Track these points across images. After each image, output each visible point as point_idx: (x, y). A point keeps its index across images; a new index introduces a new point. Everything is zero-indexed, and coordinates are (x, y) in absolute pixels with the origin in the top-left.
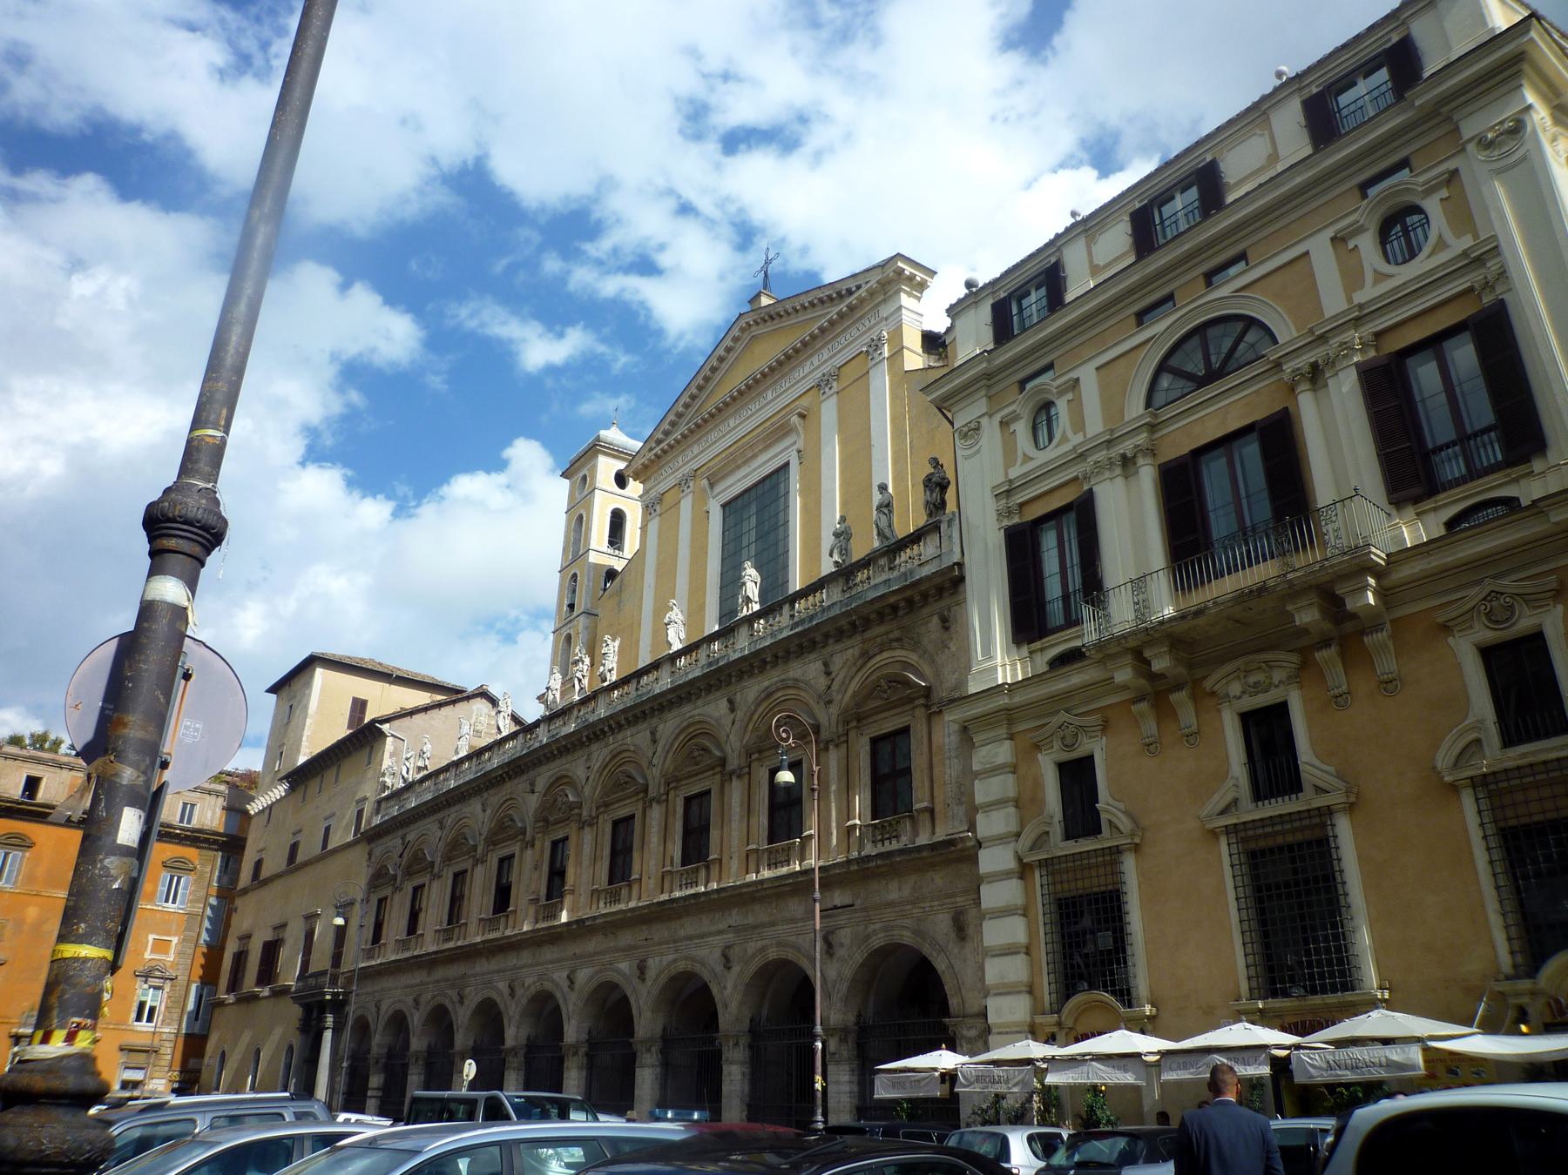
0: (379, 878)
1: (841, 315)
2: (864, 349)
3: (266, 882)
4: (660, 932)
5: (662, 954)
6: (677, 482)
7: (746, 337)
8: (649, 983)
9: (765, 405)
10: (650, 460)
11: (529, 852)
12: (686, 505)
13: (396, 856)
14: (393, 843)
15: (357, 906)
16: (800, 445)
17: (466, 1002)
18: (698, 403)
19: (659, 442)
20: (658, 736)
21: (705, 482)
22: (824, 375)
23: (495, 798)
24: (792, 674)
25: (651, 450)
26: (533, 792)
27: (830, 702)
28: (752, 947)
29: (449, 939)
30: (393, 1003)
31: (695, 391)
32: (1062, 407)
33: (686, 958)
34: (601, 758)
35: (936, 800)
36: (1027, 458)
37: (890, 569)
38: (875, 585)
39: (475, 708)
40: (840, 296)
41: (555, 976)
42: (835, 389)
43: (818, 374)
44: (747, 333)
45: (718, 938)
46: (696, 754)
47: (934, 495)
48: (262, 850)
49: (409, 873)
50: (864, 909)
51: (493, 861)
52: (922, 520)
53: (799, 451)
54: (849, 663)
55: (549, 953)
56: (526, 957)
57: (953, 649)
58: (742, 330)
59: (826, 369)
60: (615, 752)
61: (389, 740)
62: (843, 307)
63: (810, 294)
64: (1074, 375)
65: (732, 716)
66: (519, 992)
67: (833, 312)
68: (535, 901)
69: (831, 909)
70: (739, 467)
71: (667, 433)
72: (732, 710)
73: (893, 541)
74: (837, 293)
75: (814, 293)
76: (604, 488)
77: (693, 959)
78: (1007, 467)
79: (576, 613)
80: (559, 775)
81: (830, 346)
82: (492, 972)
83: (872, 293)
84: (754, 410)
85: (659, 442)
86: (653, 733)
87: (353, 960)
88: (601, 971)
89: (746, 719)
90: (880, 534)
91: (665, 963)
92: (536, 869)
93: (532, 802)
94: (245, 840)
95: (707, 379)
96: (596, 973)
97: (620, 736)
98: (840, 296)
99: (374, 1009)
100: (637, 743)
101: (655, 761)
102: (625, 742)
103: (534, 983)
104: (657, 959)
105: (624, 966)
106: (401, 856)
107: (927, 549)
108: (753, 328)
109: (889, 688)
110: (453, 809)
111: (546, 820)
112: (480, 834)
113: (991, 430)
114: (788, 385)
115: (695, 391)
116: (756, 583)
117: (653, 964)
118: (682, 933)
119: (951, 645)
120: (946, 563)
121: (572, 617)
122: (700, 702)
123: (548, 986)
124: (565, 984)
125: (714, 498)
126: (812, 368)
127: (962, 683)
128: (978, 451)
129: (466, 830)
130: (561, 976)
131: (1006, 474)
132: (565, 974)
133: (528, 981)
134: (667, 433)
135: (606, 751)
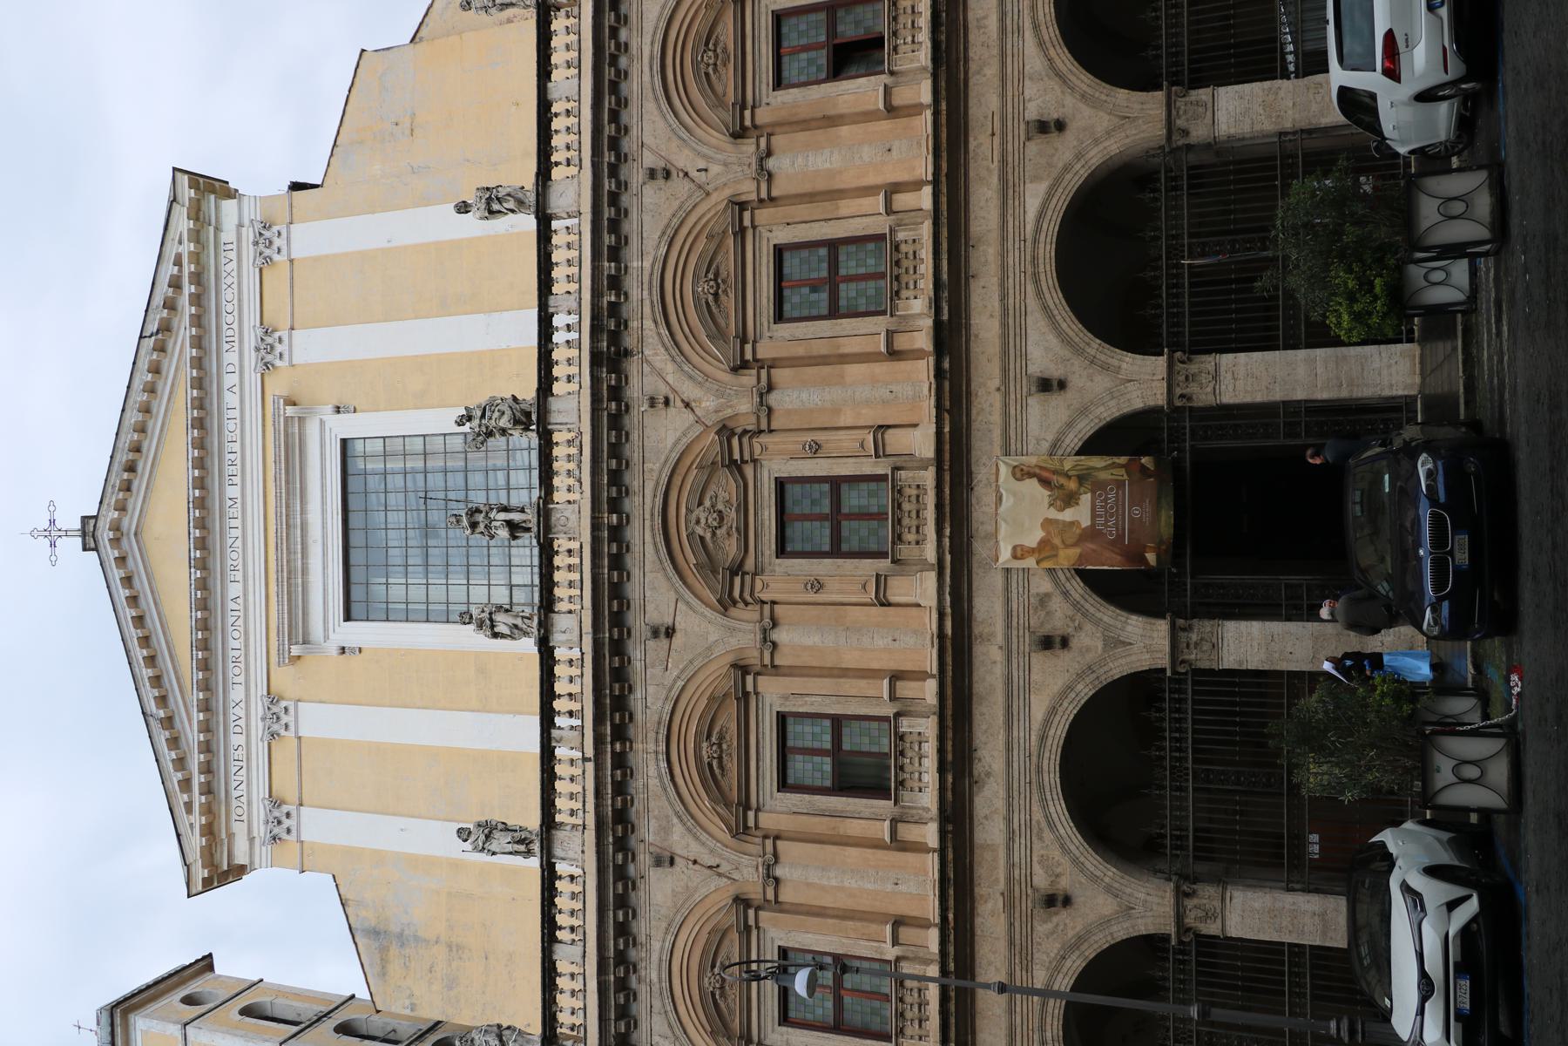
1: (197, 299)
2: (259, 261)
4: (984, 100)
6: (267, 737)
7: (129, 544)
16: (329, 408)
17: (1064, 884)
18: (170, 679)
19: (186, 784)
21: (295, 650)
22: (257, 349)
25: (189, 807)
26: (670, 632)
31: (149, 672)
40: (170, 305)
42: (284, 334)
43: (251, 358)
44: (124, 542)
53: (338, 410)
58: (116, 542)
59: (251, 340)
60: (658, 308)
62: (188, 289)
63: (140, 364)
66: (1059, 617)
67: (187, 309)
70: (305, 571)
71: (180, 763)
74: (164, 307)
75: (143, 352)
80: (658, 520)
81: (226, 346)
83: (196, 236)
85: (186, 784)
86: (652, 174)
88: (1037, 281)
95: (145, 641)
96: (1039, 294)
97: (635, 294)
98: (170, 305)
104: (1030, 90)
108: (125, 523)
111: (737, 569)
114: (236, 447)
115: (149, 672)
117: (1041, 99)
118: (993, 23)
125: (326, 638)
126: (236, 389)
132: (1035, 404)
134: (180, 763)
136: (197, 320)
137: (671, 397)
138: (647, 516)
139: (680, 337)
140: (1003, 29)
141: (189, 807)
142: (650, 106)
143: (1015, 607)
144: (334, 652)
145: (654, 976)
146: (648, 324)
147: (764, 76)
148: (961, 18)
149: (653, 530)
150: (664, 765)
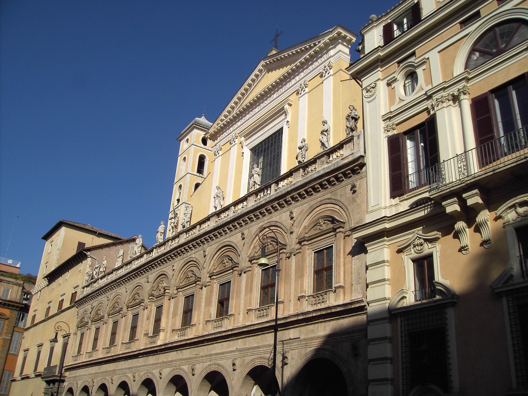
0: (82, 325)
3: (36, 325)
5: (203, 362)
8: (196, 376)
9: (273, 100)
10: (217, 129)
11: (146, 311)
12: (235, 150)
13: (89, 313)
14: (88, 306)
15: (72, 336)
17: (114, 382)
20: (207, 253)
23: (131, 285)
24: (274, 219)
25: (218, 124)
26: (148, 282)
27: (291, 233)
28: (248, 359)
29: (108, 353)
30: (84, 382)
32: (420, 72)
33: (215, 364)
34: (180, 265)
35: (346, 282)
36: (402, 100)
37: (327, 163)
38: (318, 171)
39: (130, 246)
41: (154, 372)
45: (231, 354)
46: (225, 261)
47: (351, 123)
48: (36, 310)
49: (94, 321)
50: (305, 340)
51: (130, 316)
52: (343, 136)
54: (304, 212)
55: (152, 359)
56: (141, 361)
57: (358, 201)
61: (89, 259)
64: (426, 56)
65: (244, 241)
68: (146, 335)
69: (288, 340)
72: (243, 239)
73: (329, 148)
76: (196, 144)
77: (218, 365)
78: (391, 105)
79: (180, 203)
82: (126, 369)
84: (267, 103)
87: (69, 361)
88: (174, 369)
89: (250, 243)
90: (323, 144)
91: (205, 367)
92: (148, 320)
93: (148, 287)
94: (29, 306)
96: (173, 370)
99: (75, 384)
100: (197, 257)
101: (205, 266)
102: (191, 256)
103: (144, 374)
105: (185, 368)
106: (90, 313)
107: (345, 152)
109: (324, 223)
110: (113, 291)
112: (124, 303)
113: (382, 86)
116: (259, 175)
119: (357, 200)
120: (357, 156)
121: (178, 205)
122: (228, 235)
123: (150, 376)
124: (158, 375)
126: (296, 82)
127: (361, 220)
128: (375, 98)
129: (119, 301)
130: (156, 372)
131: (390, 109)
132: (158, 371)
133: (142, 373)
135: (182, 261)
136: (307, 60)
137: (175, 270)
138: (161, 270)
139: (184, 269)
140: (210, 355)
141: (218, 124)
142: (217, 244)
143: (139, 368)
144: (242, 152)
145: (118, 292)
146: (185, 259)
147: (220, 280)
148: (214, 342)
149: (158, 273)
150: (136, 286)
